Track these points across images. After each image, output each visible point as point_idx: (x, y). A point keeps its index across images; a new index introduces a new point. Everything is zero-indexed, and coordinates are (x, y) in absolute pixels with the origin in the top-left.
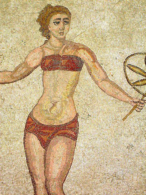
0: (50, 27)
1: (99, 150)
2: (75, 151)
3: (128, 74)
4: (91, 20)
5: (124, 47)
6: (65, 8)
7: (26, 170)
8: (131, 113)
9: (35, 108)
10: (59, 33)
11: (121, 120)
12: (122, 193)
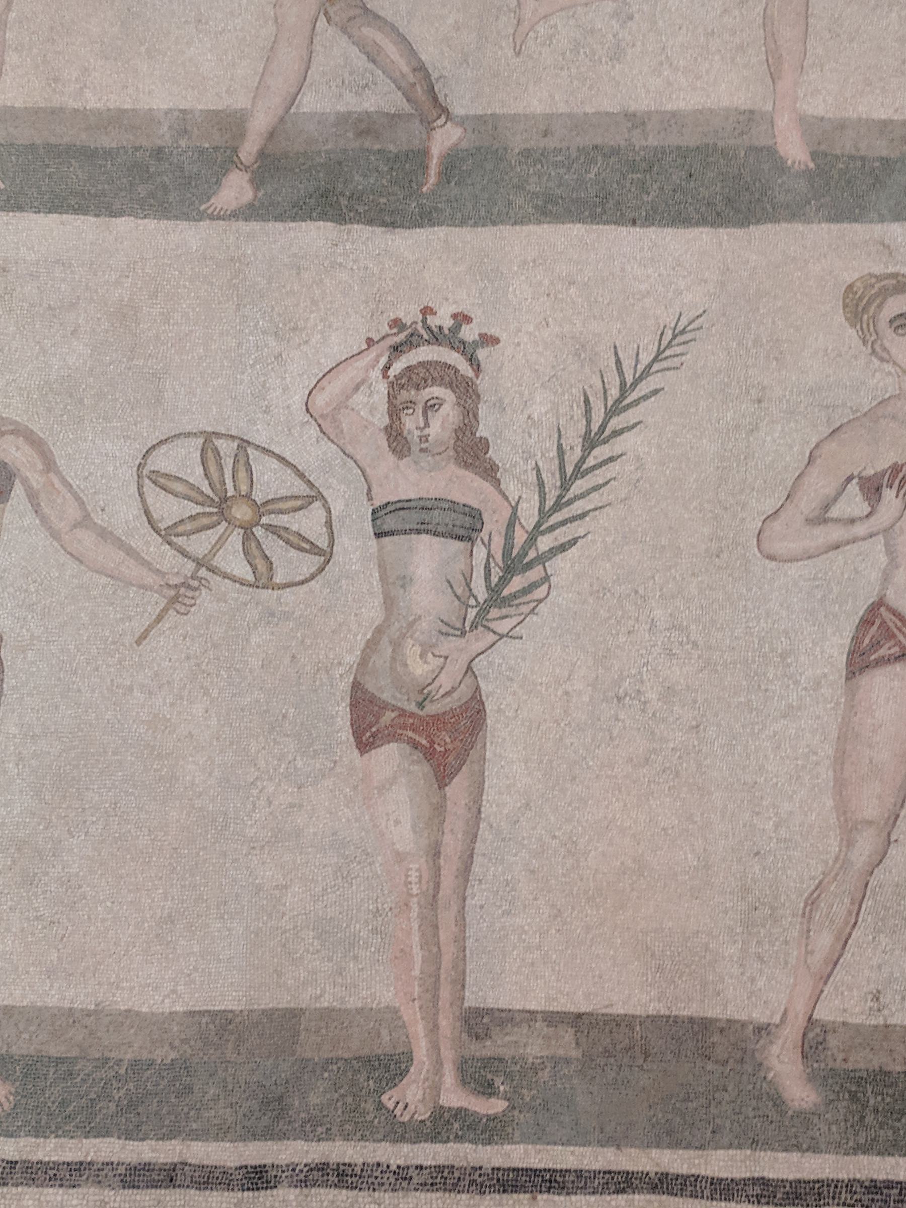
3: (150, 501)
8: (159, 619)
11: (131, 645)
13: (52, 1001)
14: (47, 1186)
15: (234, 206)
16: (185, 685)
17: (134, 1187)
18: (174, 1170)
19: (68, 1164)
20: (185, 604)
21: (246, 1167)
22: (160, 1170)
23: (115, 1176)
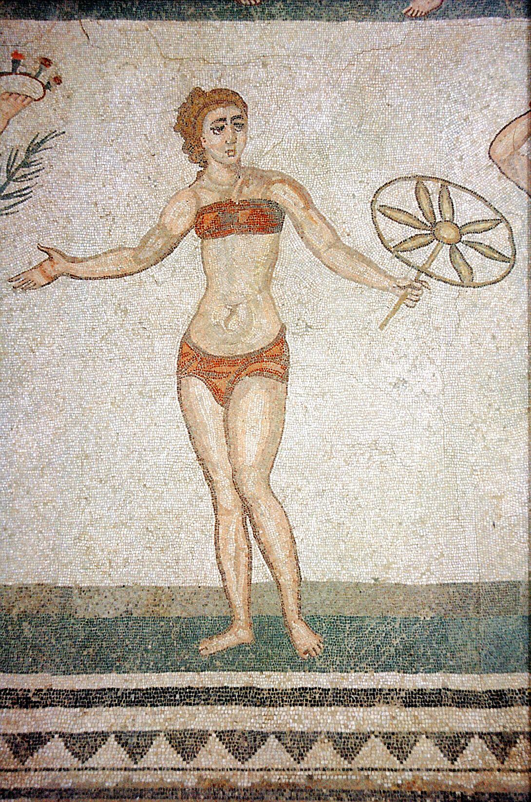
0: (205, 142)
1: (335, 397)
2: (287, 404)
3: (381, 227)
4: (292, 114)
5: (369, 169)
6: (234, 93)
7: (190, 455)
8: (395, 310)
9: (194, 322)
10: (226, 152)
12: (393, 482)
13: (344, 578)
14: (352, 705)
15: (428, 8)
16: (417, 357)
17: (412, 706)
18: (440, 694)
19: (365, 690)
20: (411, 300)
21: (490, 691)
22: (430, 694)
23: (398, 698)
